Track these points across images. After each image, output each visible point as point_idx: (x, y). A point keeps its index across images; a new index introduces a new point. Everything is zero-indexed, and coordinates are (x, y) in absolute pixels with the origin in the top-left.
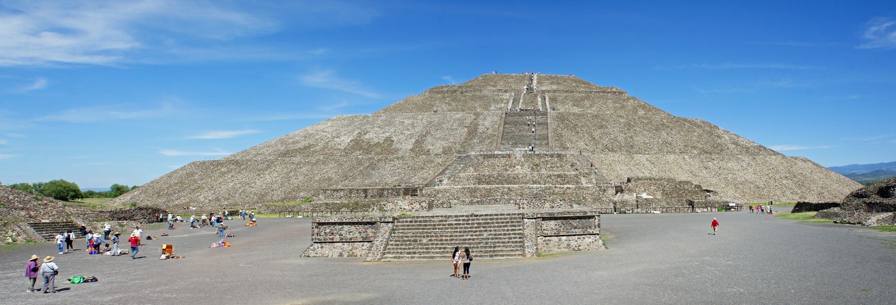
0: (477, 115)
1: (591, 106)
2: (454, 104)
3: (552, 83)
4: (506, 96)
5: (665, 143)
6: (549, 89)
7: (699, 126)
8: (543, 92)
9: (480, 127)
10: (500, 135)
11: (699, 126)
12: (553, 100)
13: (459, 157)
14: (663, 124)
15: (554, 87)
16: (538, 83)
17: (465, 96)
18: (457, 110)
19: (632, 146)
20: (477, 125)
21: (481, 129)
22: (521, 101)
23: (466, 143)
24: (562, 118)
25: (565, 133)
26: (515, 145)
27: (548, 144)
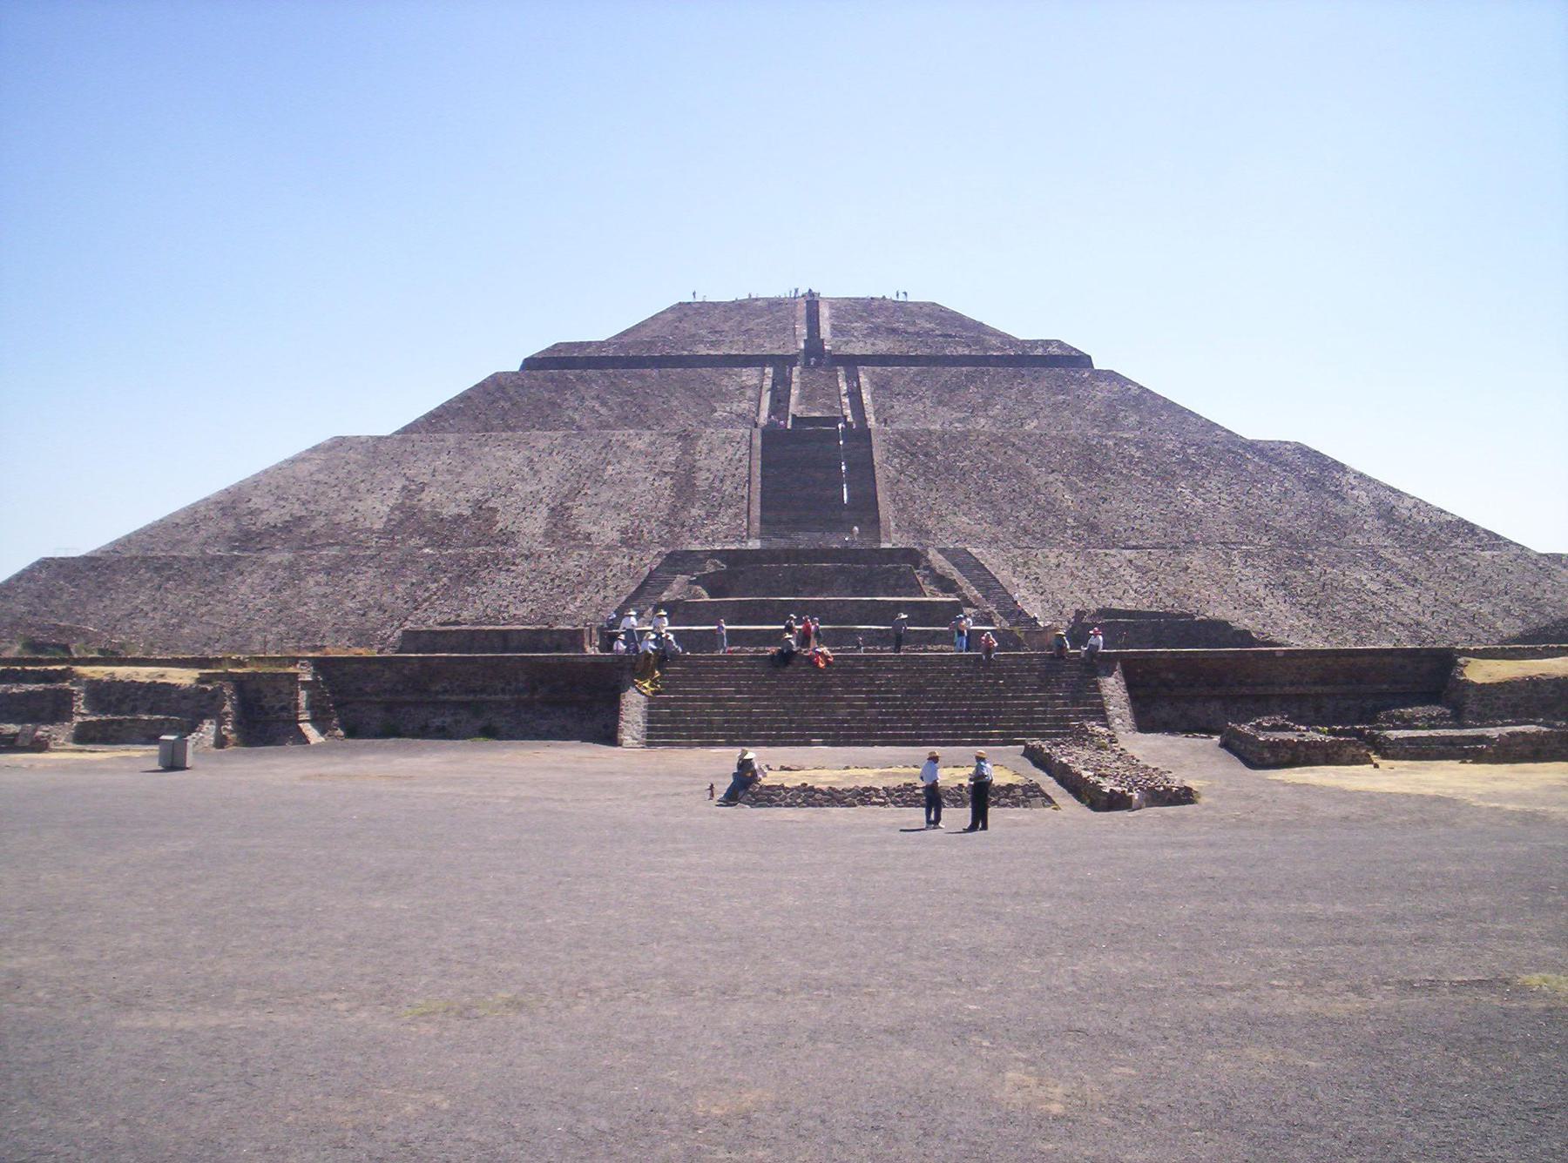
0: (686, 437)
1: (987, 403)
2: (613, 400)
3: (874, 331)
4: (749, 376)
5: (1183, 517)
6: (868, 350)
7: (1284, 465)
8: (852, 363)
9: (704, 475)
10: (756, 498)
11: (1284, 465)
12: (880, 386)
13: (669, 556)
14: (1186, 461)
15: (883, 346)
16: (836, 331)
17: (642, 378)
18: (624, 421)
19: (1093, 528)
20: (692, 469)
21: (702, 480)
22: (795, 391)
23: (673, 520)
24: (910, 447)
25: (917, 490)
26: (797, 524)
27: (877, 520)
